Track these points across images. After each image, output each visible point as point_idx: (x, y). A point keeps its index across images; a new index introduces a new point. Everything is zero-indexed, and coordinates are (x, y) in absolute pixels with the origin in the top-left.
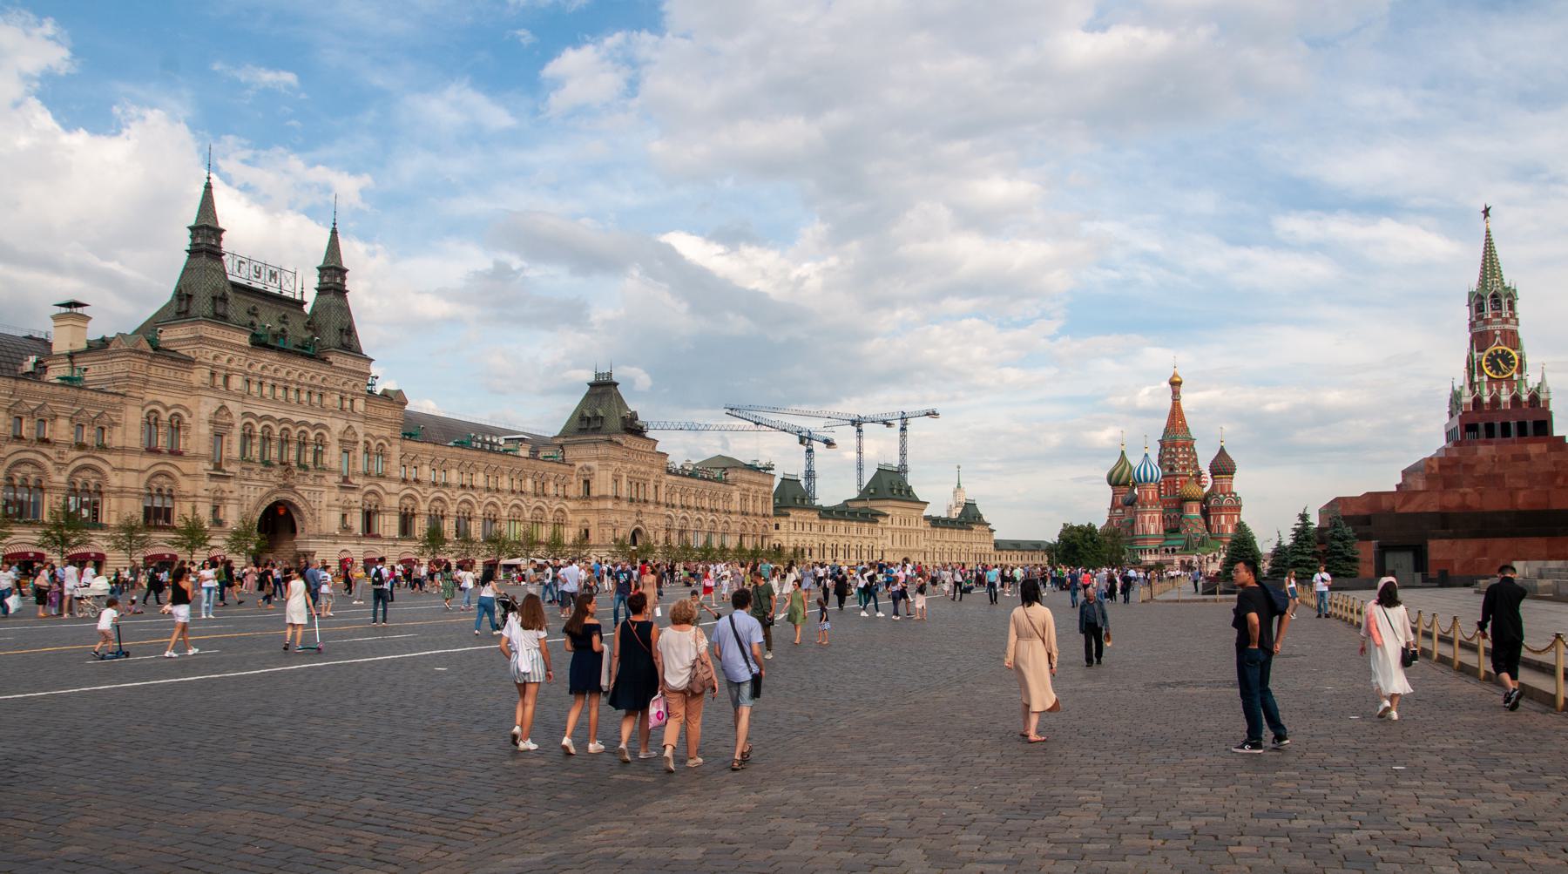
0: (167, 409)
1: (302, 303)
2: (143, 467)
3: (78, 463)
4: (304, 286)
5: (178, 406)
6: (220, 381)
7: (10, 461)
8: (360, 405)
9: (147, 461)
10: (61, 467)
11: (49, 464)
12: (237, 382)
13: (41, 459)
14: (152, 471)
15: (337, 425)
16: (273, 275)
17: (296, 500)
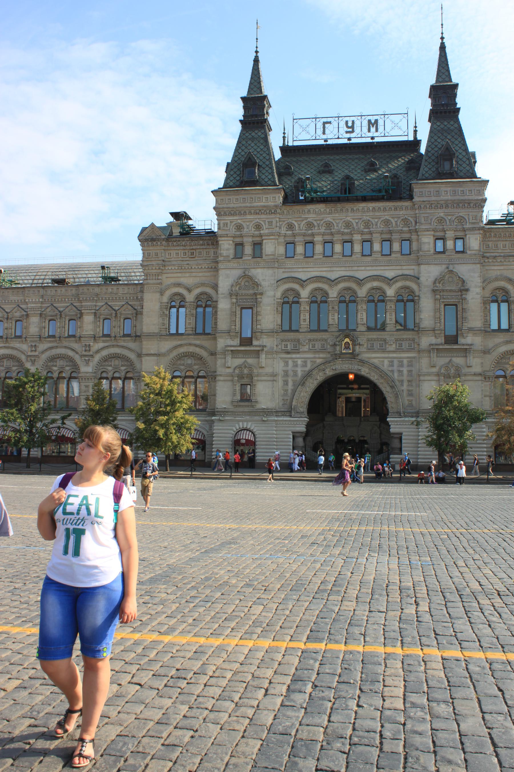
0: (189, 290)
1: (416, 143)
2: (163, 351)
3: (105, 353)
4: (410, 120)
5: (203, 285)
6: (248, 250)
7: (44, 357)
8: (474, 242)
9: (166, 345)
10: (88, 358)
11: (77, 358)
12: (270, 247)
13: (71, 353)
14: (175, 353)
15: (430, 273)
16: (373, 124)
17: (365, 372)
